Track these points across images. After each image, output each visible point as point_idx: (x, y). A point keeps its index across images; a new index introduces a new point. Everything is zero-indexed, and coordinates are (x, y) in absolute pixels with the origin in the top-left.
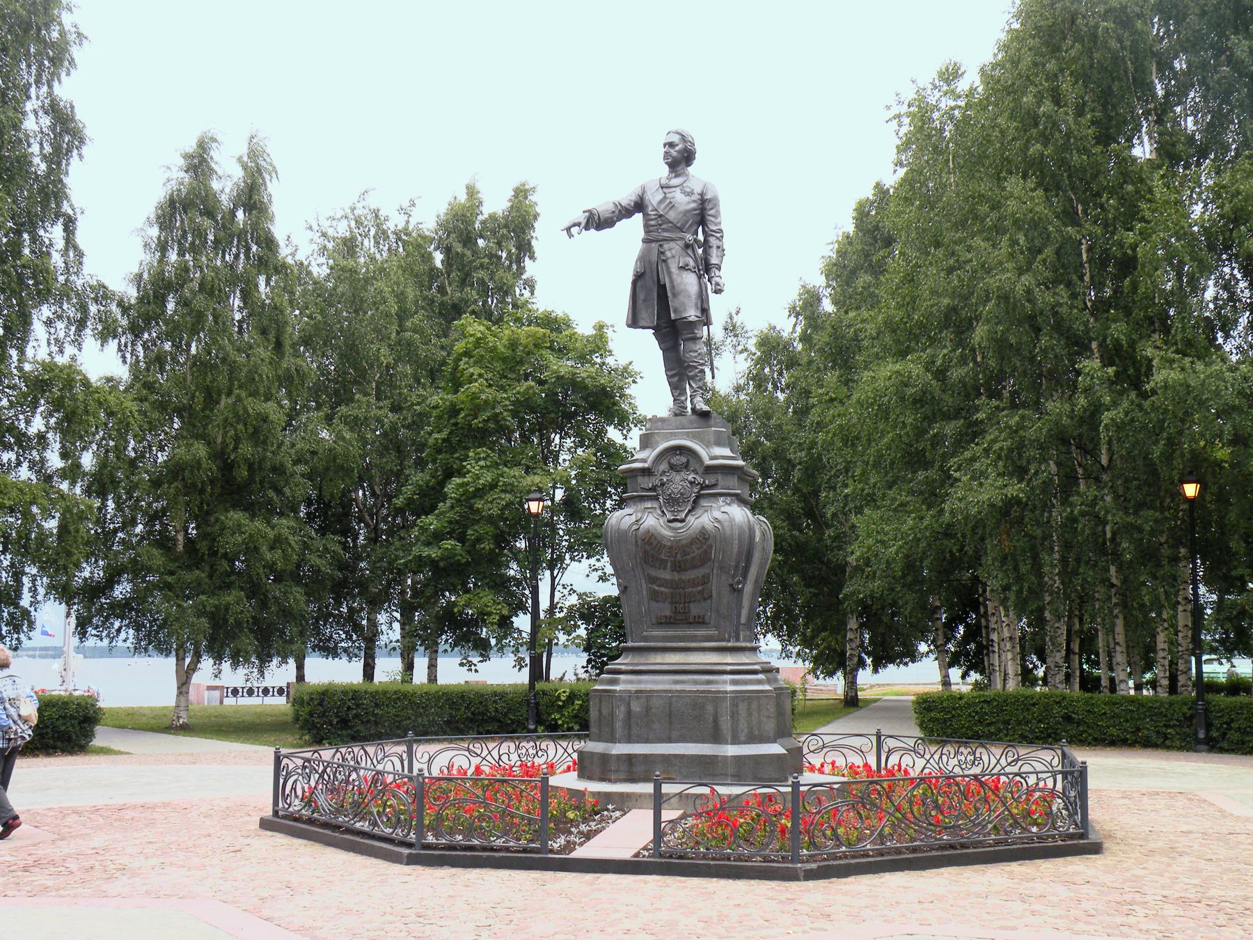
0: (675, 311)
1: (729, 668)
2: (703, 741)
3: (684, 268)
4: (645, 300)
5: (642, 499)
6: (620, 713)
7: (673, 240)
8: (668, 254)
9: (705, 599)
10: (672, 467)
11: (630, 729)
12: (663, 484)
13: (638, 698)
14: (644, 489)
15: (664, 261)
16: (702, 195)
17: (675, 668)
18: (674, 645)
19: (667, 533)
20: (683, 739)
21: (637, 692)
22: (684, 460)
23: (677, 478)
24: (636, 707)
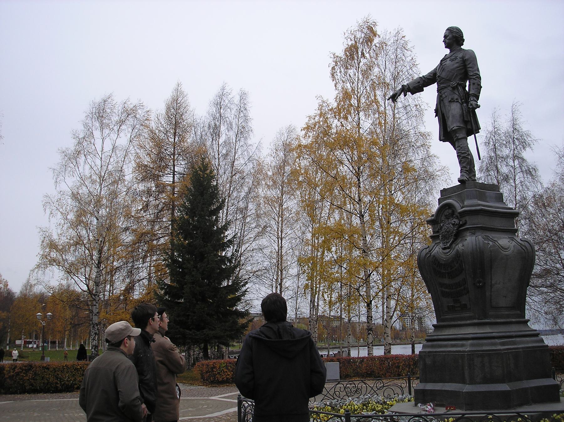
8: (444, 96)
16: (463, 58)
18: (459, 322)
20: (451, 381)
21: (429, 352)
22: (450, 211)
24: (428, 361)
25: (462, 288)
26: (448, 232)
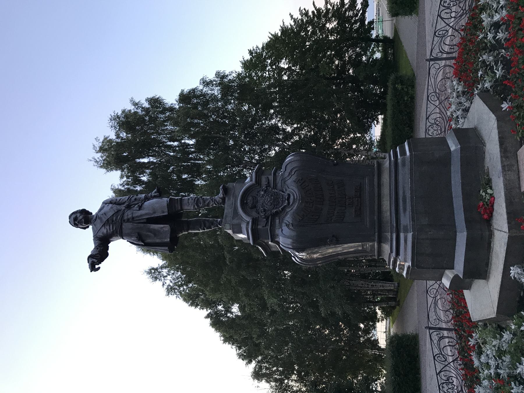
5: (273, 226)
7: (123, 214)
8: (130, 216)
10: (254, 207)
12: (265, 210)
17: (393, 178)
26: (272, 196)
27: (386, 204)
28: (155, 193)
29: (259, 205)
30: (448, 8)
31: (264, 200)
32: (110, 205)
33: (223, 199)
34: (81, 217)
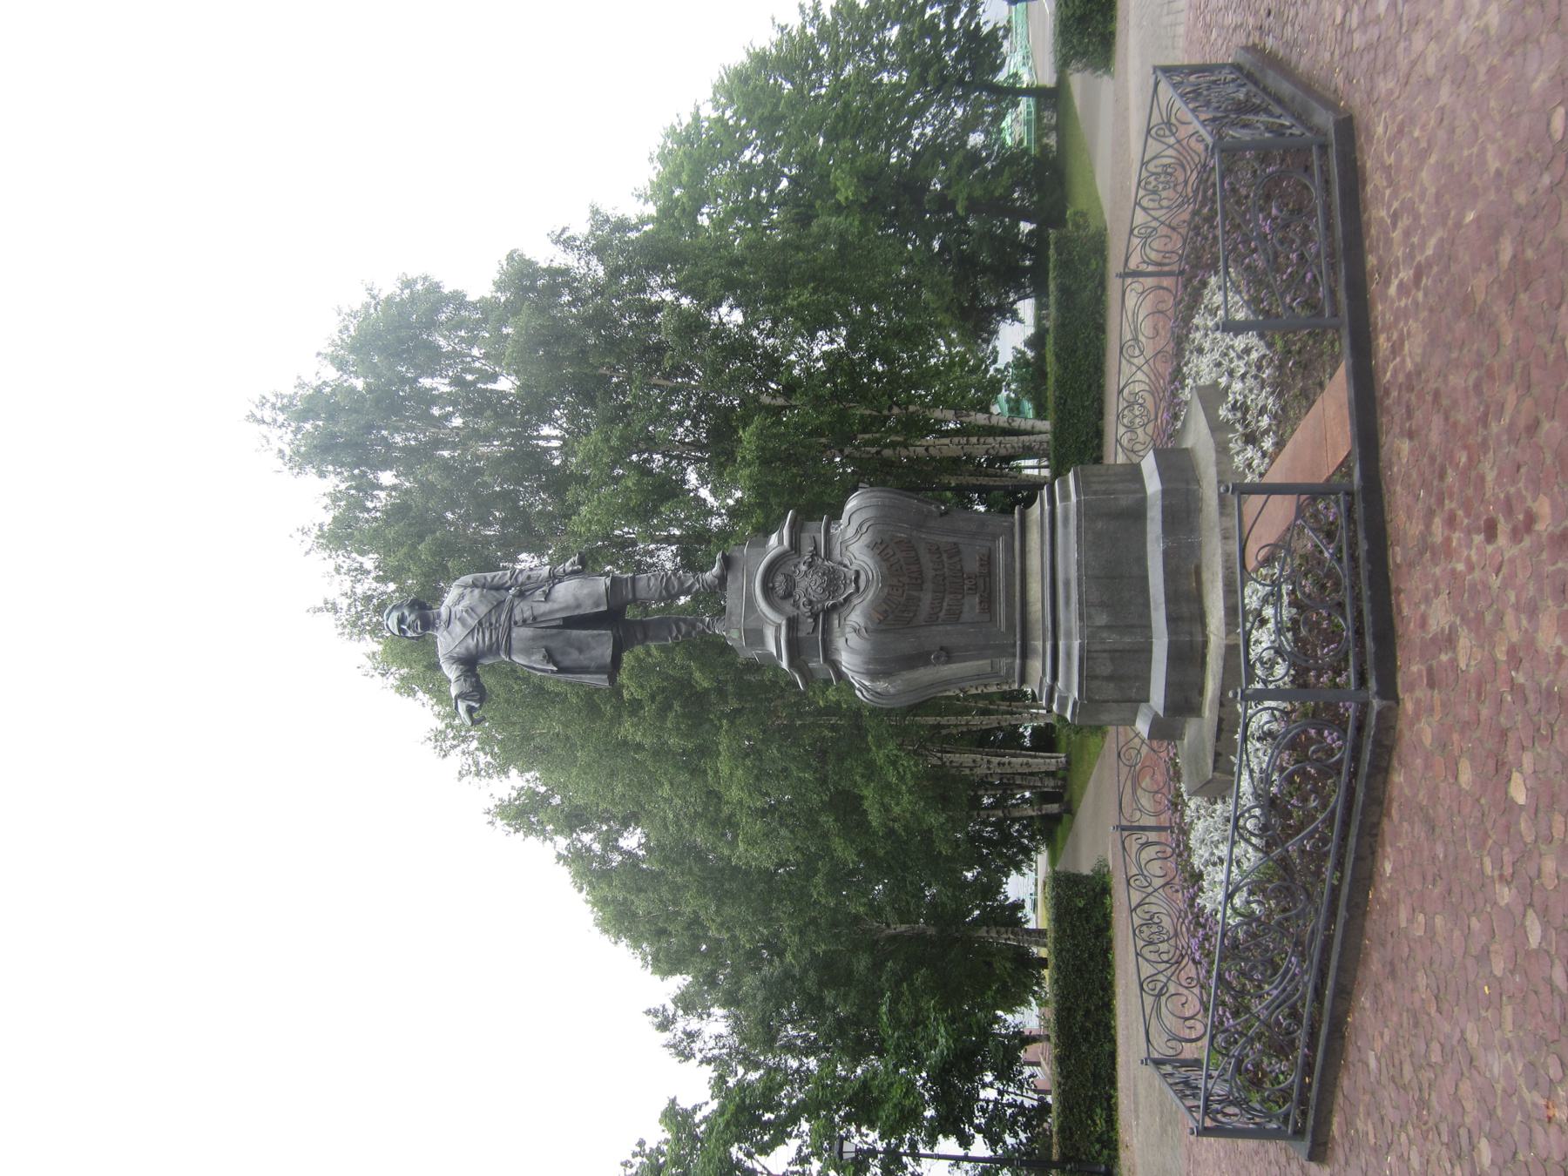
0: (598, 605)
1: (1047, 507)
2: (1143, 533)
3: (547, 596)
4: (581, 651)
5: (827, 631)
6: (1111, 639)
7: (511, 610)
8: (527, 614)
9: (959, 552)
10: (788, 595)
11: (1133, 626)
13: (1090, 617)
14: (815, 628)
15: (535, 618)
18: (1018, 594)
19: (870, 595)
20: (1142, 560)
23: (802, 584)
25: (945, 557)
27: (1036, 590)
28: (573, 564)
29: (799, 591)
30: (1154, 192)
31: (809, 584)
32: (477, 591)
33: (722, 579)
34: (412, 617)
